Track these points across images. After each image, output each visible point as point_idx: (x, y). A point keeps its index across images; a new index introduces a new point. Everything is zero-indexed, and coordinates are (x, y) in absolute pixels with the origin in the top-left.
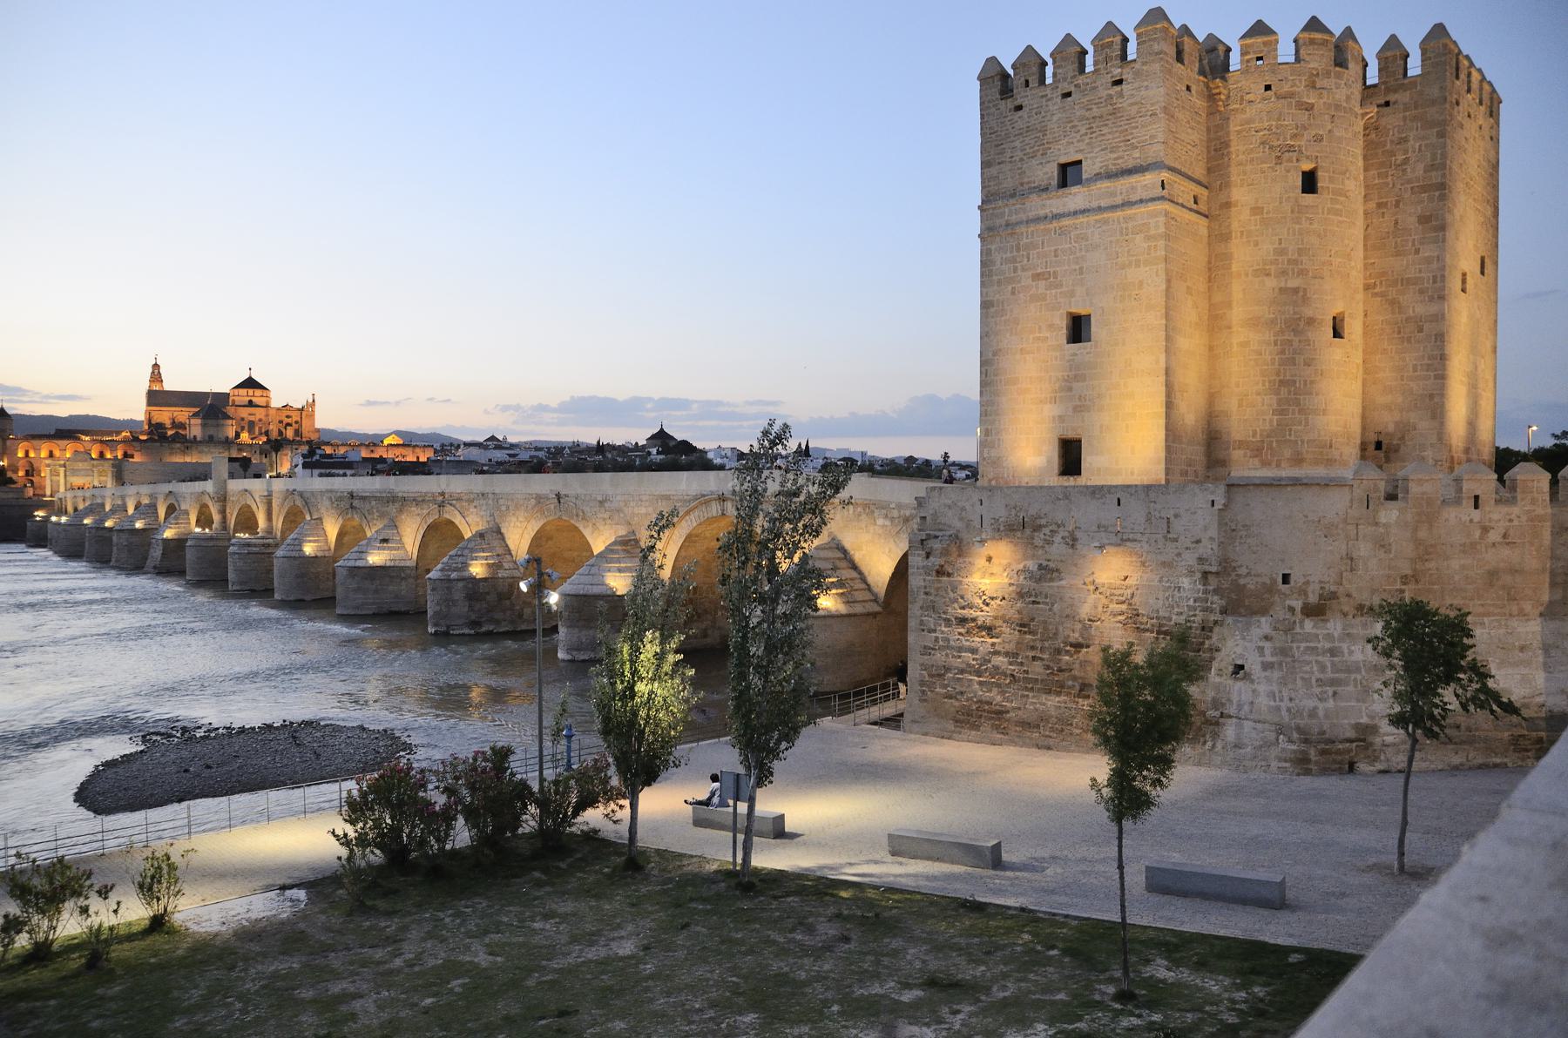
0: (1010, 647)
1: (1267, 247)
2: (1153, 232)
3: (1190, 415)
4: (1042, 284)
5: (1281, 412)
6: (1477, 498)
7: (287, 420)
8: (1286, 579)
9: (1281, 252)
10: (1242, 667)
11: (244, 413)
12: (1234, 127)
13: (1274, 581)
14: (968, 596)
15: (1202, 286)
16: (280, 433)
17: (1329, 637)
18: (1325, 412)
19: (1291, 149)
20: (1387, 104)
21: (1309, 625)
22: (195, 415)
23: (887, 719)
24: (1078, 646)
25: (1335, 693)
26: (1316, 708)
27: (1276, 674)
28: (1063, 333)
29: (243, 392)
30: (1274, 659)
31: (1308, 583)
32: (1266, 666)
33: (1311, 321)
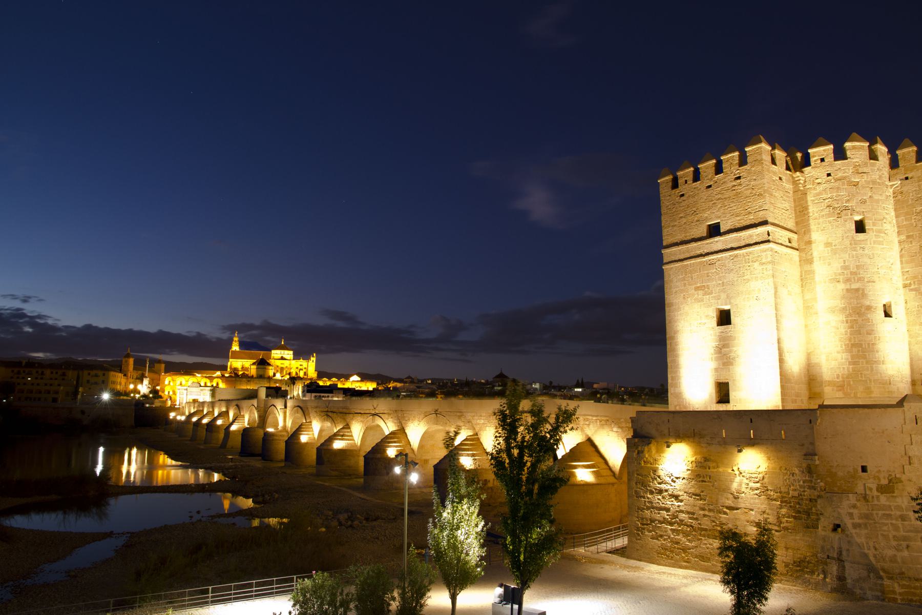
0: (689, 509)
1: (837, 265)
2: (764, 261)
3: (795, 365)
4: (701, 292)
5: (854, 363)
8: (864, 469)
9: (845, 268)
10: (839, 526)
11: (279, 363)
12: (810, 198)
13: (856, 471)
14: (663, 476)
15: (797, 289)
17: (898, 508)
20: (907, 178)
21: (883, 500)
22: (254, 364)
23: (617, 550)
24: (731, 508)
25: (908, 547)
26: (895, 555)
27: (864, 532)
28: (714, 321)
30: (860, 521)
31: (879, 471)
32: (855, 526)
33: (869, 308)
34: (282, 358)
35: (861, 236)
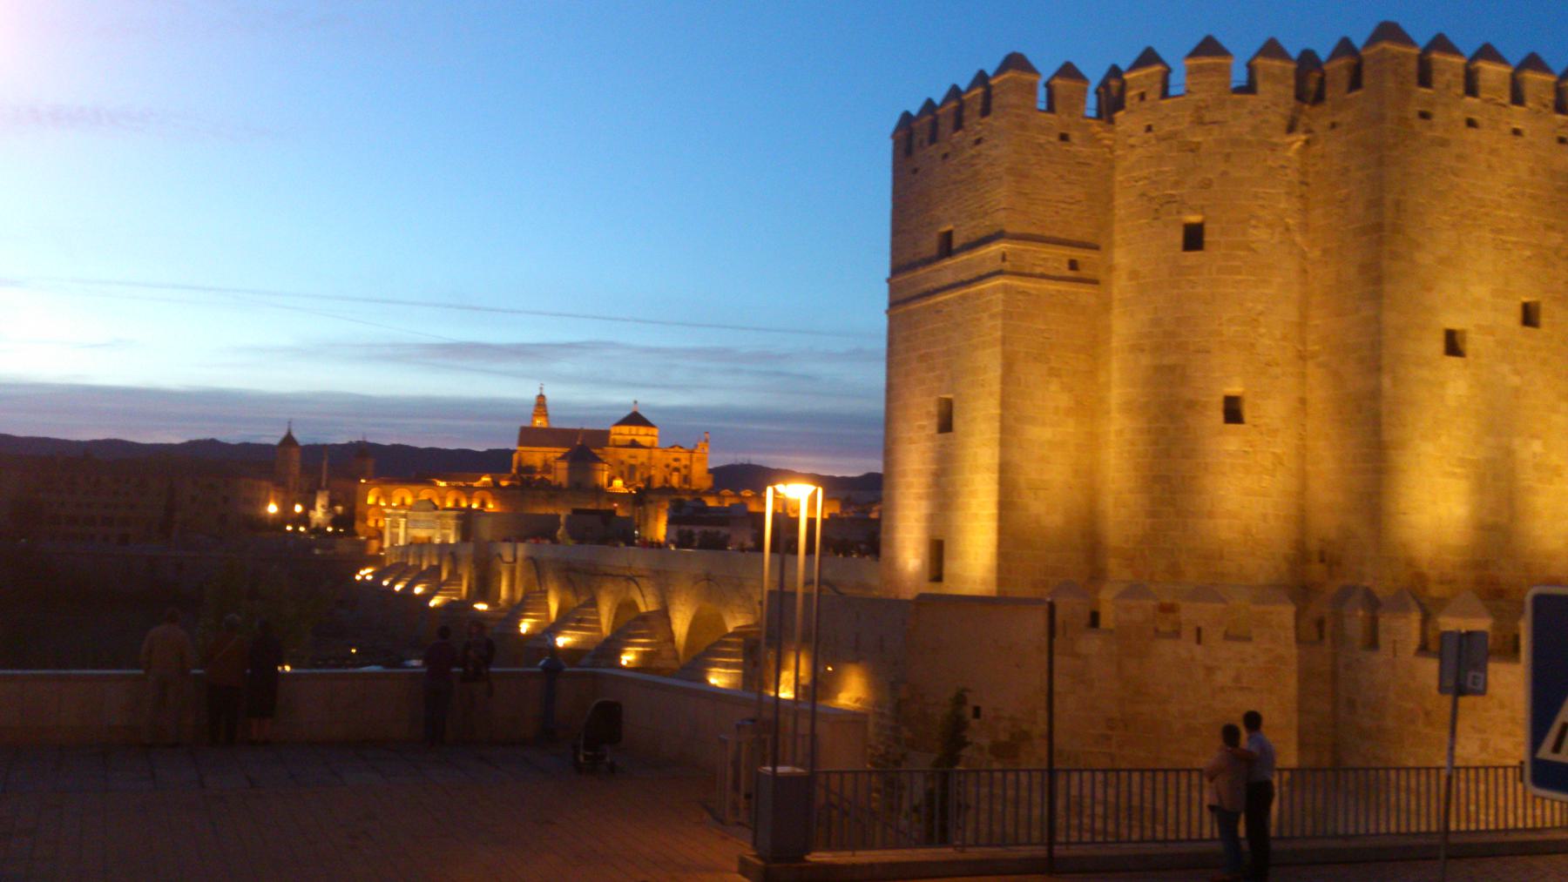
6: (1199, 630)
7: (676, 464)
9: (1156, 322)
11: (625, 454)
16: (666, 480)
18: (1211, 515)
19: (1171, 200)
20: (1333, 126)
22: (563, 458)
29: (625, 429)
33: (1191, 405)
34: (634, 444)
35: (1193, 257)
